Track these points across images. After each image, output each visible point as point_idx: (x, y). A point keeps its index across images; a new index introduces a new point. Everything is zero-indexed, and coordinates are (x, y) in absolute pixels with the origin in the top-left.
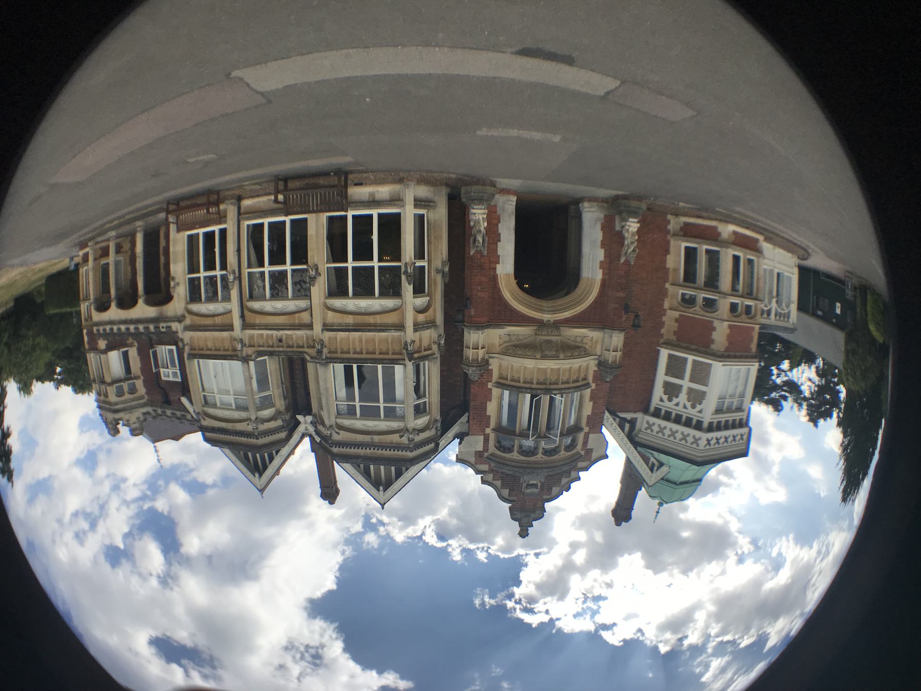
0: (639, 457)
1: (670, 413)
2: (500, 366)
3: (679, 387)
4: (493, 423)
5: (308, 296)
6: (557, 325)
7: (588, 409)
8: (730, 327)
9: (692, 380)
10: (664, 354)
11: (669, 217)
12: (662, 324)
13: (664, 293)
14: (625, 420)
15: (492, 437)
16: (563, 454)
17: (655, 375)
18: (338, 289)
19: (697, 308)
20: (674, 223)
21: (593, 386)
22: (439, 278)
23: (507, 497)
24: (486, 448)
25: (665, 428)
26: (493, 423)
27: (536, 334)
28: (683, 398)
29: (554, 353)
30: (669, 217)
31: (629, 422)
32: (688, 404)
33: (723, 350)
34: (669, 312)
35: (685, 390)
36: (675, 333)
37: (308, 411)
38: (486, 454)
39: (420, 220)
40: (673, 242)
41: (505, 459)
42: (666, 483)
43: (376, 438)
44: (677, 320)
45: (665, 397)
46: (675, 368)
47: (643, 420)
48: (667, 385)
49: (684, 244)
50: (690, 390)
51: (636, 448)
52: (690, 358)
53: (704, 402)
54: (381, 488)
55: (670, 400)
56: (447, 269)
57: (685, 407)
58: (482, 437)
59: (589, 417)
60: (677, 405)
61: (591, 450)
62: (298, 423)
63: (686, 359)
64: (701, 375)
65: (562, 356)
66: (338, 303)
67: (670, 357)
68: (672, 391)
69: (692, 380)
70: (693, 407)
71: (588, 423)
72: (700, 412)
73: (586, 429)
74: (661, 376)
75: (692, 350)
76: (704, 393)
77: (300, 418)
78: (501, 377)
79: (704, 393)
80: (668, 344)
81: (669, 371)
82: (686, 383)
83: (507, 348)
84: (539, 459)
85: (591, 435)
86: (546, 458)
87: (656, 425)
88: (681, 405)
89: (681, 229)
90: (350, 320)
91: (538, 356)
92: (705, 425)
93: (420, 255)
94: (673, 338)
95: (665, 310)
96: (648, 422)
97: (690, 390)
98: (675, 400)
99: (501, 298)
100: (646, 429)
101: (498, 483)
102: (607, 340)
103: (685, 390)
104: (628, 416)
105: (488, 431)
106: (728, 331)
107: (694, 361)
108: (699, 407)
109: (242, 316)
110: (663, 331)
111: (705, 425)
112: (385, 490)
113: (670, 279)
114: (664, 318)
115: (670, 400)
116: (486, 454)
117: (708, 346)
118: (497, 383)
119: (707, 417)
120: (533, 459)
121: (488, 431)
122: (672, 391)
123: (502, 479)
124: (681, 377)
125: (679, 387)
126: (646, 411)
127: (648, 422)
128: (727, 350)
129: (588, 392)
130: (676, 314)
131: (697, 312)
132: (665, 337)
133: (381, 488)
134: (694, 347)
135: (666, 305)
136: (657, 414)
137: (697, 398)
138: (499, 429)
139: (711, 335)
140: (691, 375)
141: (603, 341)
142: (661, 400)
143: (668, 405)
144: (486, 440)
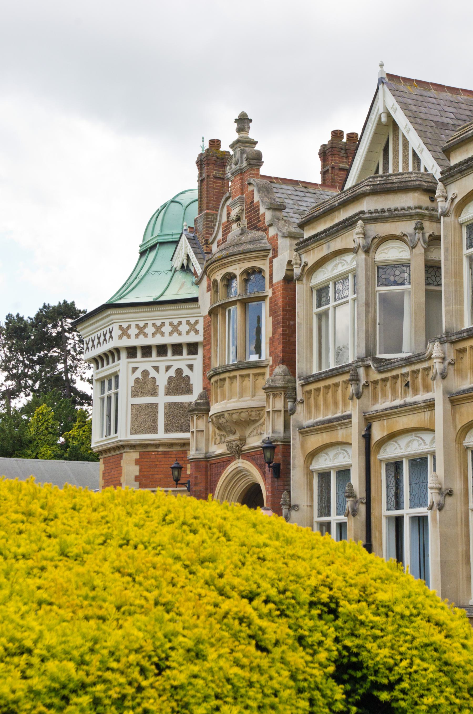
1: (174, 354)
3: (169, 392)
24: (271, 262)
25: (171, 334)
27: (243, 440)
28: (162, 380)
29: (220, 421)
32: (153, 373)
33: (124, 455)
35: (161, 390)
50: (154, 393)
52: (161, 435)
53: (132, 384)
55: (179, 371)
57: (157, 369)
60: (168, 368)
64: (144, 417)
68: (180, 384)
69: (154, 407)
72: (134, 370)
76: (135, 395)
82: (162, 400)
84: (218, 273)
87: (184, 332)
88: (162, 369)
91: (226, 415)
92: (123, 355)
97: (154, 393)
98: (172, 373)
101: (262, 210)
102: (202, 445)
103: (161, 390)
107: (155, 431)
108: (138, 374)
111: (123, 355)
115: (179, 371)
118: (266, 366)
119: (123, 365)
120: (224, 271)
125: (169, 392)
128: (120, 456)
137: (144, 385)
139: (140, 471)
140: (157, 412)
141: (207, 440)
142: (191, 367)
143: (180, 362)
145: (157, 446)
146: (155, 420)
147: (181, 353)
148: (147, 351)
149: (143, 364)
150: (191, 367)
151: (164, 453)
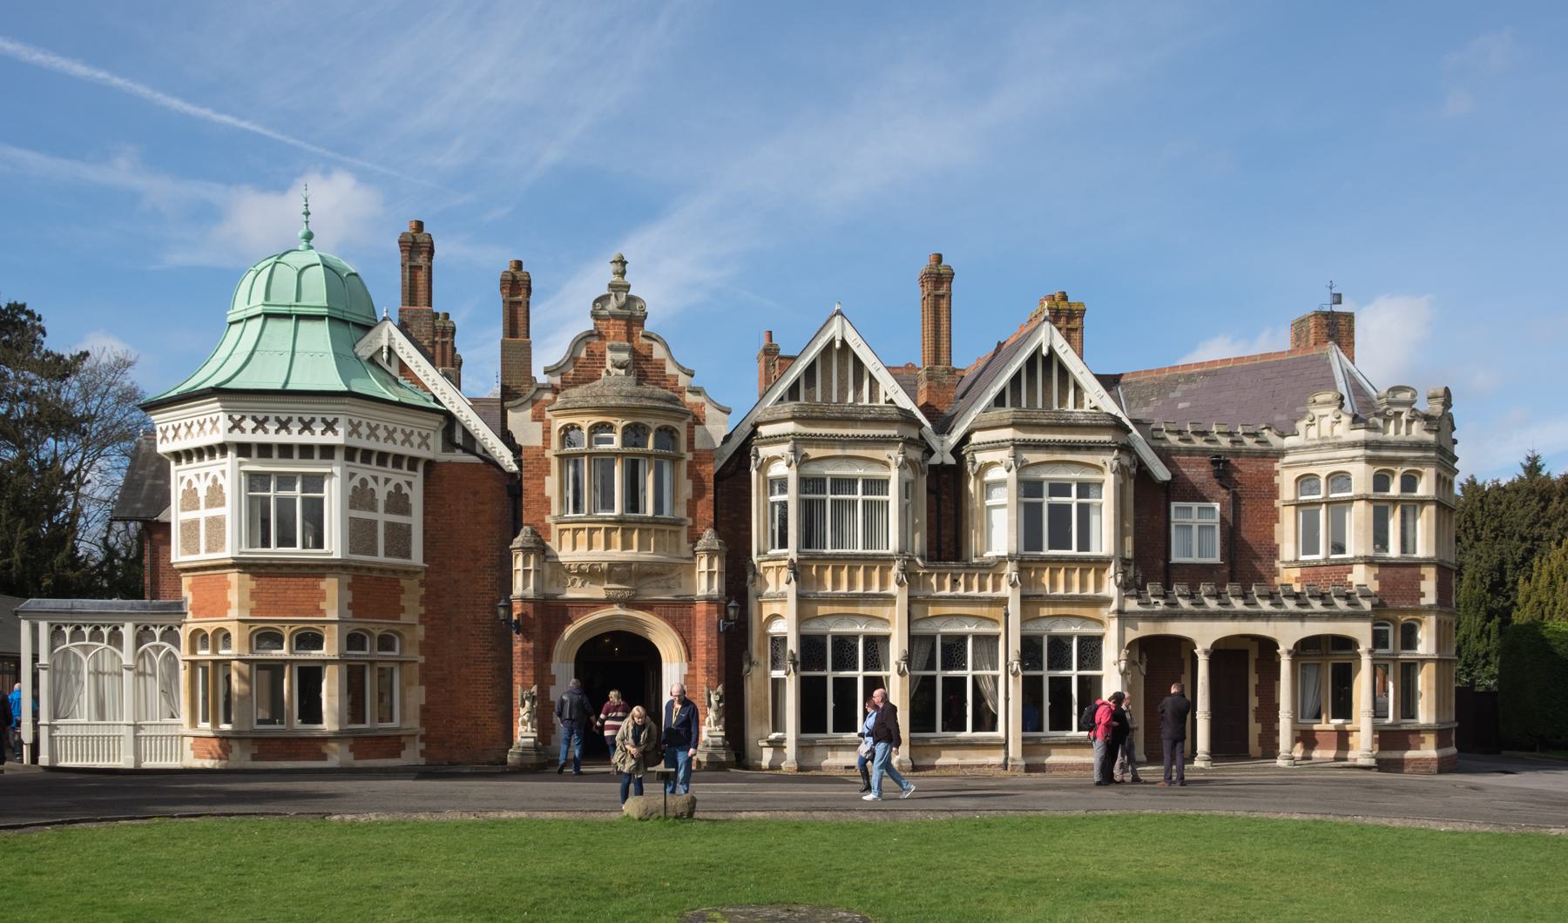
0: (424, 379)
2: (678, 546)
3: (390, 509)
4: (684, 467)
5: (912, 639)
6: (609, 602)
7: (551, 485)
8: (322, 612)
9: (374, 523)
10: (417, 558)
11: (422, 761)
12: (424, 601)
13: (424, 647)
14: (465, 450)
15: (683, 448)
16: (586, 422)
17: (425, 523)
18: (877, 646)
19: (377, 633)
20: (411, 755)
21: (549, 520)
22: (755, 656)
23: (655, 345)
24: (691, 427)
25: (403, 443)
26: (684, 467)
28: (381, 494)
30: (422, 761)
31: (458, 446)
34: (416, 621)
35: (381, 506)
36: (403, 591)
37: (938, 472)
38: (690, 419)
39: (778, 725)
40: (414, 723)
41: (666, 417)
42: (348, 317)
43: (838, 452)
44: (403, 609)
45: (405, 489)
46: (398, 539)
47: (434, 450)
48: (406, 510)
49: (396, 723)
51: (436, 400)
52: (381, 557)
54: (838, 345)
55: (398, 487)
56: (746, 667)
57: (375, 479)
58: (698, 445)
59: (548, 472)
60: (387, 481)
61: (538, 417)
62: (956, 451)
63: (387, 554)
65: (605, 565)
66: (876, 629)
67: (408, 555)
68: (398, 502)
69: (374, 523)
70: (364, 482)
71: (548, 463)
72: (352, 475)
73: (549, 454)
74: (416, 520)
75: (381, 570)
77: (951, 460)
78: (677, 533)
79: (352, 506)
80: (409, 572)
81: (406, 531)
83: (672, 571)
85: (539, 443)
86: (610, 420)
88: (381, 481)
89: (403, 747)
90: (862, 610)
93: (778, 685)
94: (404, 582)
95: (421, 623)
96: (428, 447)
98: (391, 487)
99: (681, 634)
100: (428, 436)
101: (670, 369)
104: (459, 457)
105: (689, 456)
106: (322, 606)
107: (375, 553)
108: (356, 482)
109: (1007, 615)
110: (422, 591)
112: (832, 342)
113: (416, 668)
114: (422, 610)
115: (398, 487)
116: (690, 419)
117: (354, 577)
121: (689, 456)
122: (398, 502)
123: (664, 378)
124: (388, 525)
125: (390, 509)
126: (430, 464)
127: (428, 447)
129: (555, 510)
130: (404, 618)
131: (378, 627)
132: (416, 581)
133: (838, 345)
134: (375, 574)
135: (421, 631)
136: (413, 462)
137: (359, 497)
138: (675, 460)
142: (409, 484)
143: (400, 476)
144: (691, 441)
145: (369, 569)
146: (374, 539)
147: (400, 467)
148: (367, 455)
149: (364, 471)
150: (409, 484)
151: (377, 579)
